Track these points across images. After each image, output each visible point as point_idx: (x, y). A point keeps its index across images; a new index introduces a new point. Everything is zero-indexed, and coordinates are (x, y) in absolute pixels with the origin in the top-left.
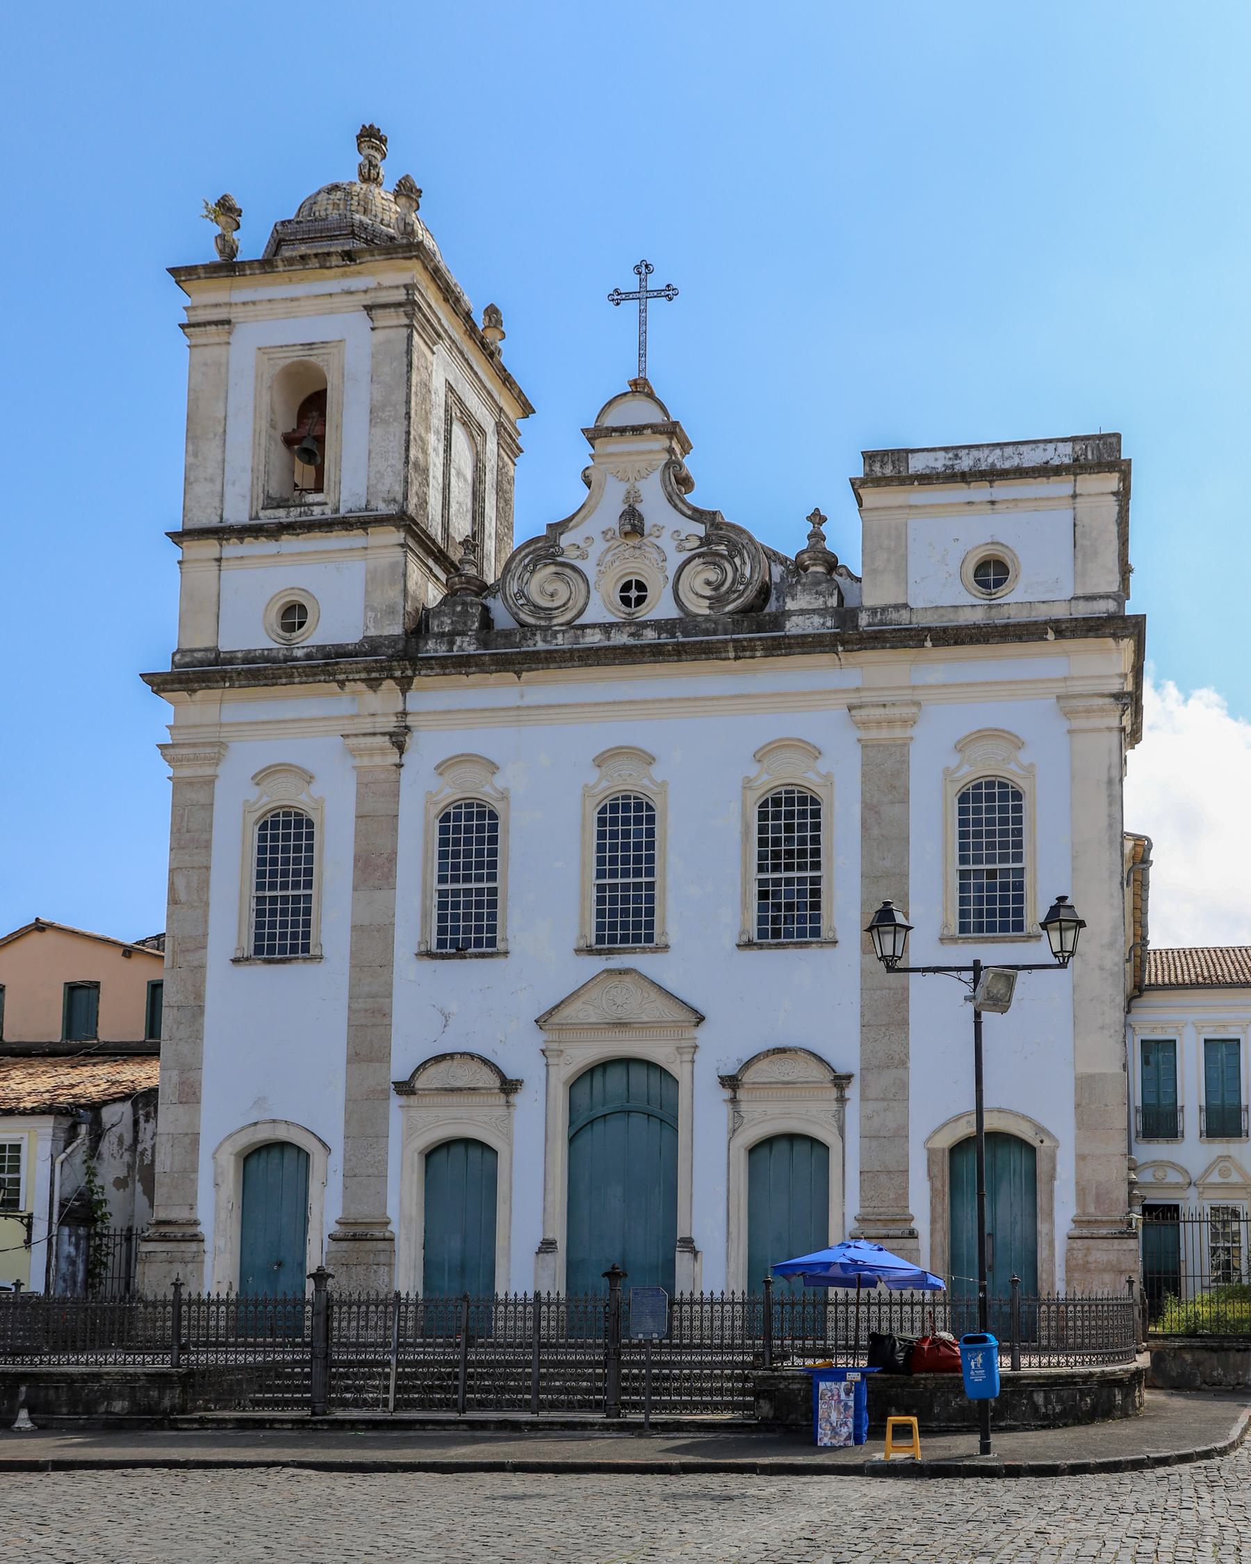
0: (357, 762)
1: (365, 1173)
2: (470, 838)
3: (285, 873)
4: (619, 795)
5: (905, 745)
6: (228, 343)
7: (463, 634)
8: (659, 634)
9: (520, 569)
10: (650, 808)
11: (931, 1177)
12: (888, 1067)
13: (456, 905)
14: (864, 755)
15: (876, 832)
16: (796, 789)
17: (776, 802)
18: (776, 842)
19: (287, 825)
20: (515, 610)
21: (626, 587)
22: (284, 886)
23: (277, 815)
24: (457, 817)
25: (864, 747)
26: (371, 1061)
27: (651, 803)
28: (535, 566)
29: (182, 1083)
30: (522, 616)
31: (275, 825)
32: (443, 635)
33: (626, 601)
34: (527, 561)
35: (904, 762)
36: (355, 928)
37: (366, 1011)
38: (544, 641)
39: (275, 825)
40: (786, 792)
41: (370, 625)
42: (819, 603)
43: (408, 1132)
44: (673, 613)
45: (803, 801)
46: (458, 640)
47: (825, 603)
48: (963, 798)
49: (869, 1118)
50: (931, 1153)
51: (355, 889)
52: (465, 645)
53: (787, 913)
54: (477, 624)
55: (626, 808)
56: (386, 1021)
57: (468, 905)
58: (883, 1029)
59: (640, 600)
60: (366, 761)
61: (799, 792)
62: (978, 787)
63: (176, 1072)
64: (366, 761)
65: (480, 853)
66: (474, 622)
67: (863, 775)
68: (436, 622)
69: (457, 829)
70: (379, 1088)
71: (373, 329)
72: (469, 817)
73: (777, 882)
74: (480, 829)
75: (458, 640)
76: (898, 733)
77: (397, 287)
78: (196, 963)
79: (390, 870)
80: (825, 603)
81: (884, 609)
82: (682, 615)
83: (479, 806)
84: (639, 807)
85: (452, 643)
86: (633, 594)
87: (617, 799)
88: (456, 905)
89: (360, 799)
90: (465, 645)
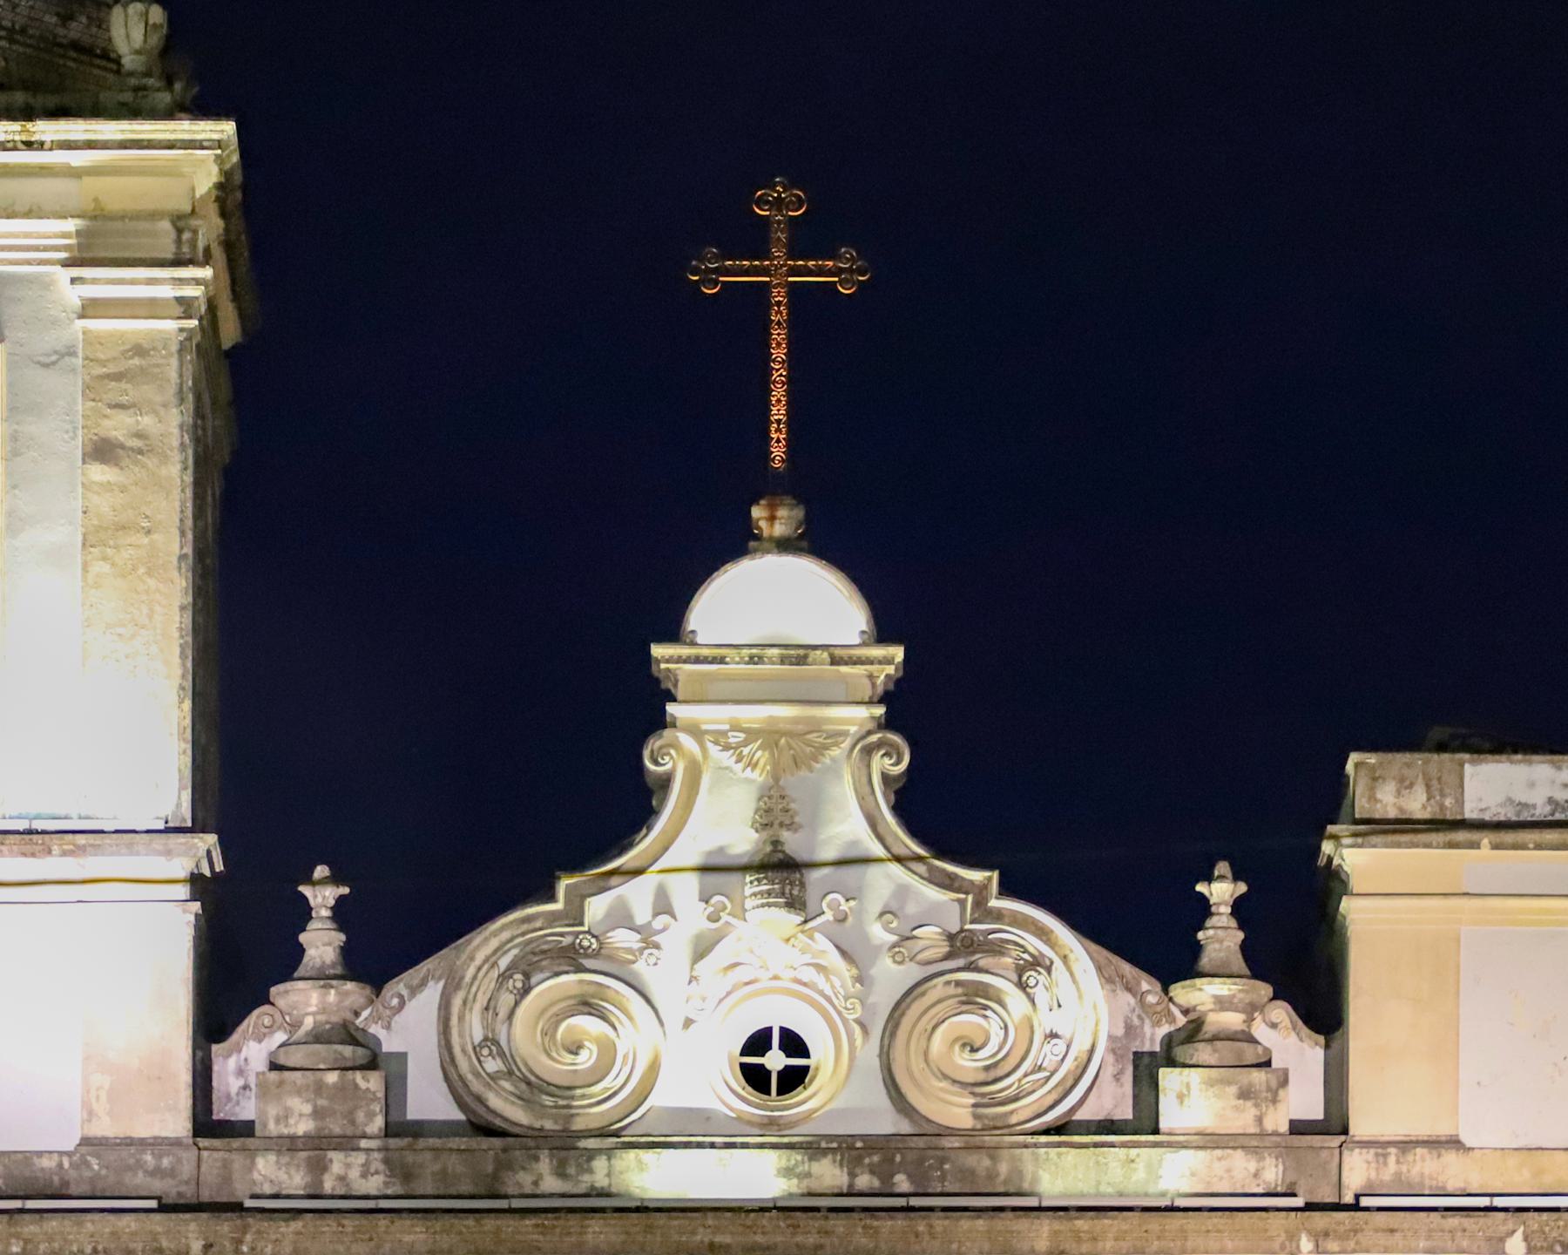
7: (347, 1143)
8: (852, 1175)
9: (489, 983)
20: (476, 1086)
21: (758, 1043)
28: (527, 976)
30: (495, 1101)
32: (289, 1145)
33: (756, 1078)
34: (504, 962)
38: (561, 1173)
41: (101, 1107)
42: (1242, 1119)
44: (887, 1122)
46: (337, 1161)
47: (1259, 1120)
52: (354, 1174)
54: (379, 1122)
59: (793, 1079)
66: (371, 1116)
68: (273, 1111)
75: (337, 1161)
77: (154, 216)
80: (1259, 1120)
81: (1405, 1145)
82: (905, 1127)
85: (318, 1167)
86: (775, 1060)
90: (354, 1174)
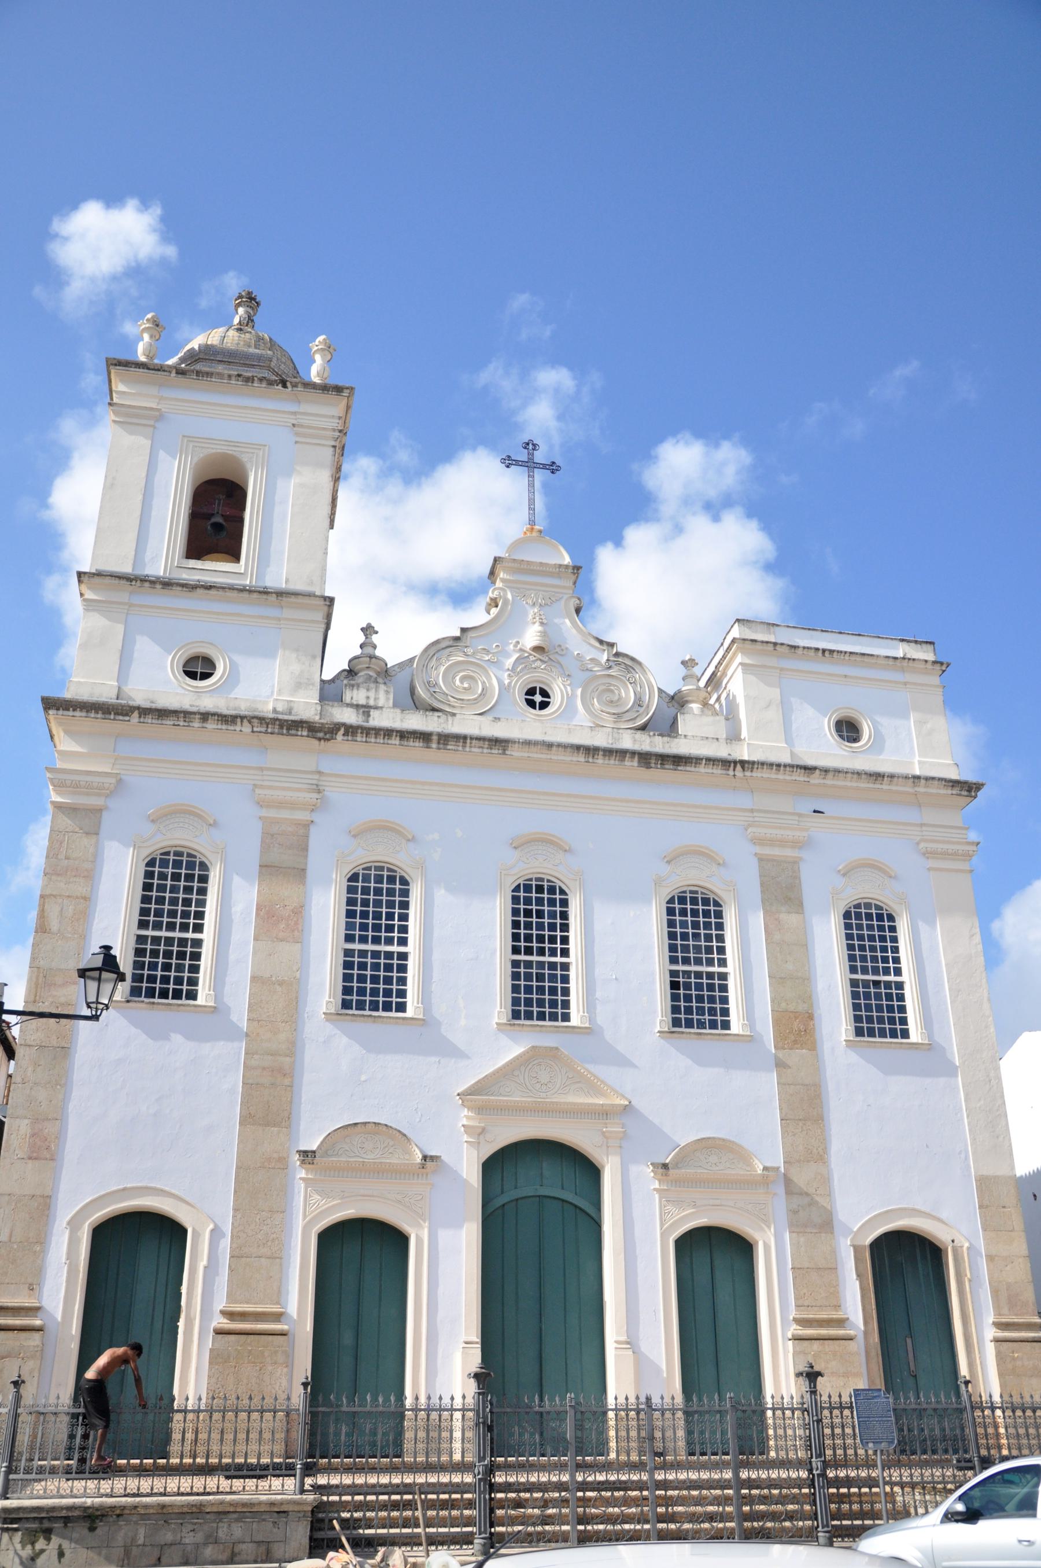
0: (264, 813)
1: (255, 1251)
2: (376, 904)
3: (172, 914)
4: (534, 876)
5: (795, 862)
6: (155, 427)
10: (562, 892)
11: (859, 1275)
12: (808, 1161)
13: (363, 966)
14: (761, 868)
15: (777, 937)
16: (699, 890)
17: (682, 900)
18: (685, 936)
19: (177, 864)
21: (531, 692)
22: (171, 927)
23: (168, 853)
24: (366, 878)
25: (760, 860)
26: (267, 1124)
27: (564, 887)
29: (33, 1135)
31: (164, 863)
35: (796, 877)
36: (254, 979)
37: (264, 1069)
39: (164, 863)
40: (691, 892)
43: (309, 1210)
45: (706, 901)
48: (847, 915)
49: (795, 1212)
50: (857, 1249)
51: (256, 939)
53: (696, 1003)
55: (540, 889)
56: (287, 1082)
57: (376, 967)
58: (801, 1124)
60: (272, 813)
61: (702, 893)
62: (858, 906)
63: (26, 1121)
64: (272, 813)
65: (390, 916)
67: (762, 885)
69: (366, 891)
70: (275, 1155)
71: (296, 442)
72: (379, 879)
73: (687, 974)
74: (391, 892)
76: (788, 852)
78: (62, 1000)
79: (296, 923)
83: (389, 870)
84: (552, 890)
87: (531, 880)
88: (363, 966)
89: (265, 847)
